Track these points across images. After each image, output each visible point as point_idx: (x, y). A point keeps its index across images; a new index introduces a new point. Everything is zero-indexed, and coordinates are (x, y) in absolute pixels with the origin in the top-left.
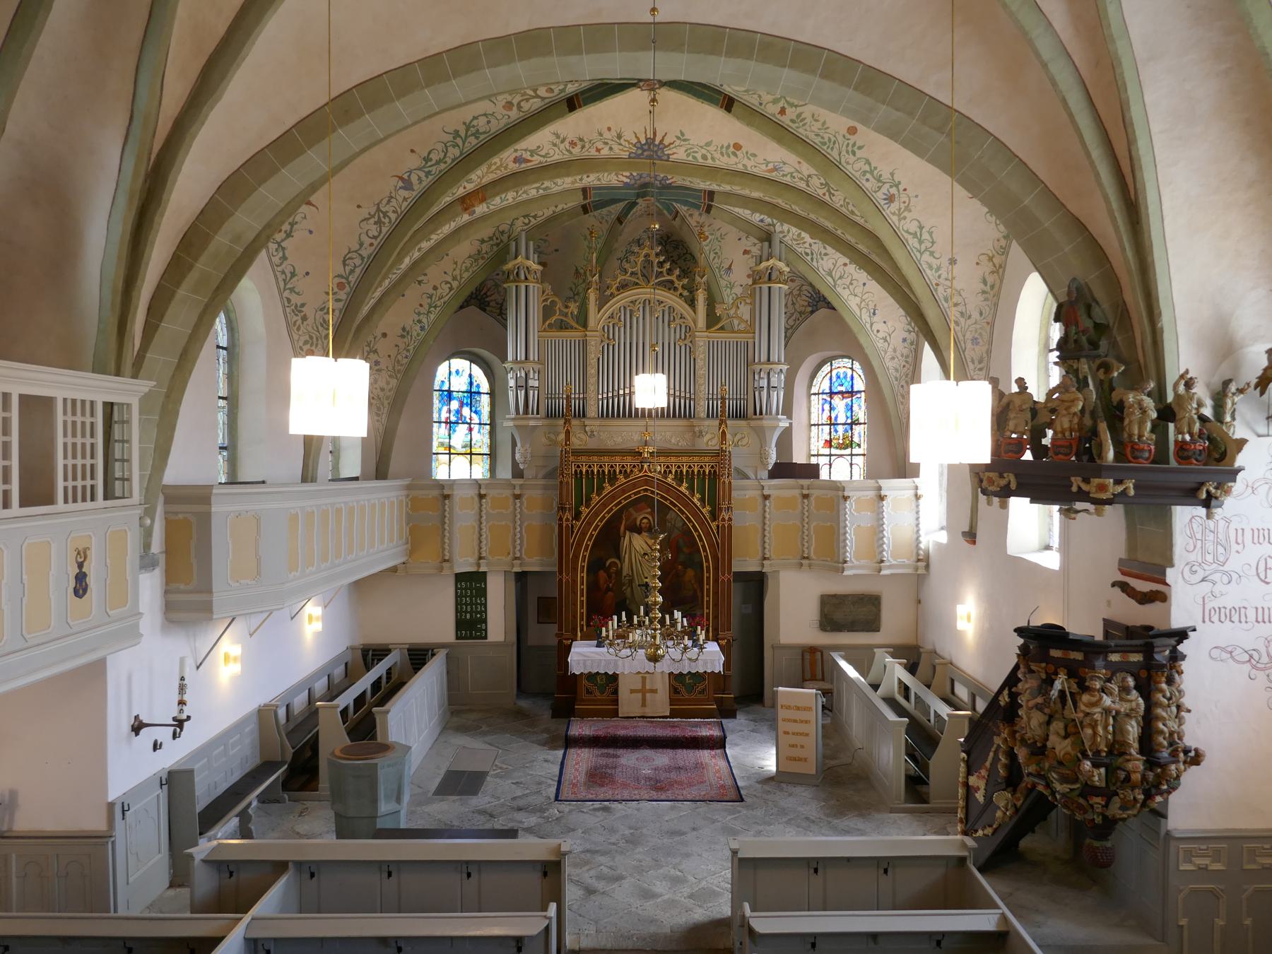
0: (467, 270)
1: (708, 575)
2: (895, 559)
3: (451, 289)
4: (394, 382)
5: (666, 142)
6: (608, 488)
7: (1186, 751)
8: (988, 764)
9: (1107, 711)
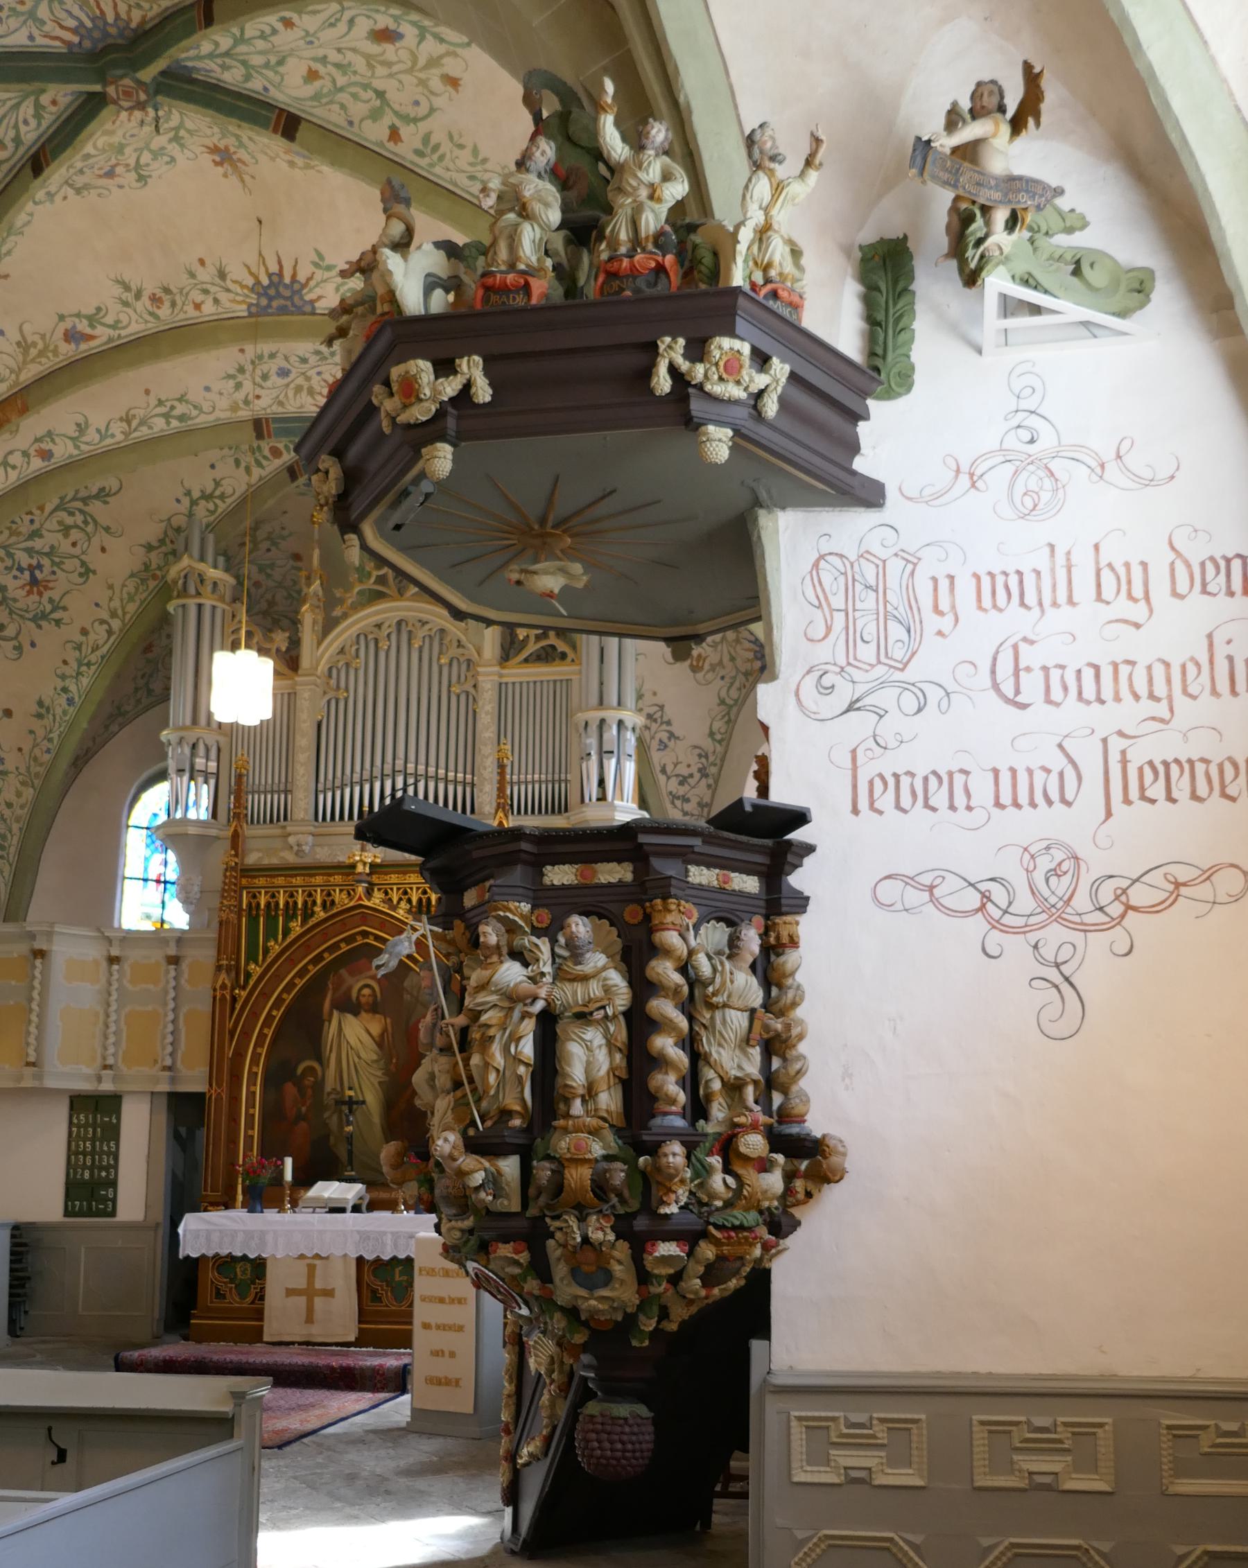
0: (131, 599)
3: (110, 632)
4: (29, 793)
5: (302, 277)
6: (296, 927)
9: (512, 998)
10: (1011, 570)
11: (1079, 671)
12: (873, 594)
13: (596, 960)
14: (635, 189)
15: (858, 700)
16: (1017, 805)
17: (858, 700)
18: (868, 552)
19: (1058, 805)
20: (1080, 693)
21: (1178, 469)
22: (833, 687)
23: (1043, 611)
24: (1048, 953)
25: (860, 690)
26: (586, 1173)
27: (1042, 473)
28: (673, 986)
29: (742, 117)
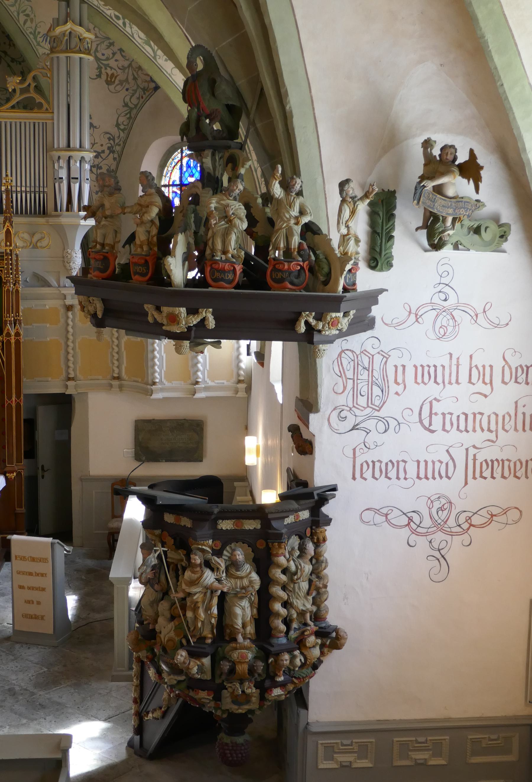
10: (431, 365)
11: (458, 416)
12: (367, 372)
13: (247, 568)
14: (289, 220)
15: (357, 425)
16: (427, 478)
17: (357, 425)
18: (365, 350)
19: (445, 479)
20: (458, 427)
21: (510, 321)
22: (346, 417)
23: (444, 386)
24: (435, 545)
25: (359, 419)
26: (246, 667)
27: (449, 317)
28: (283, 582)
29: (316, 115)
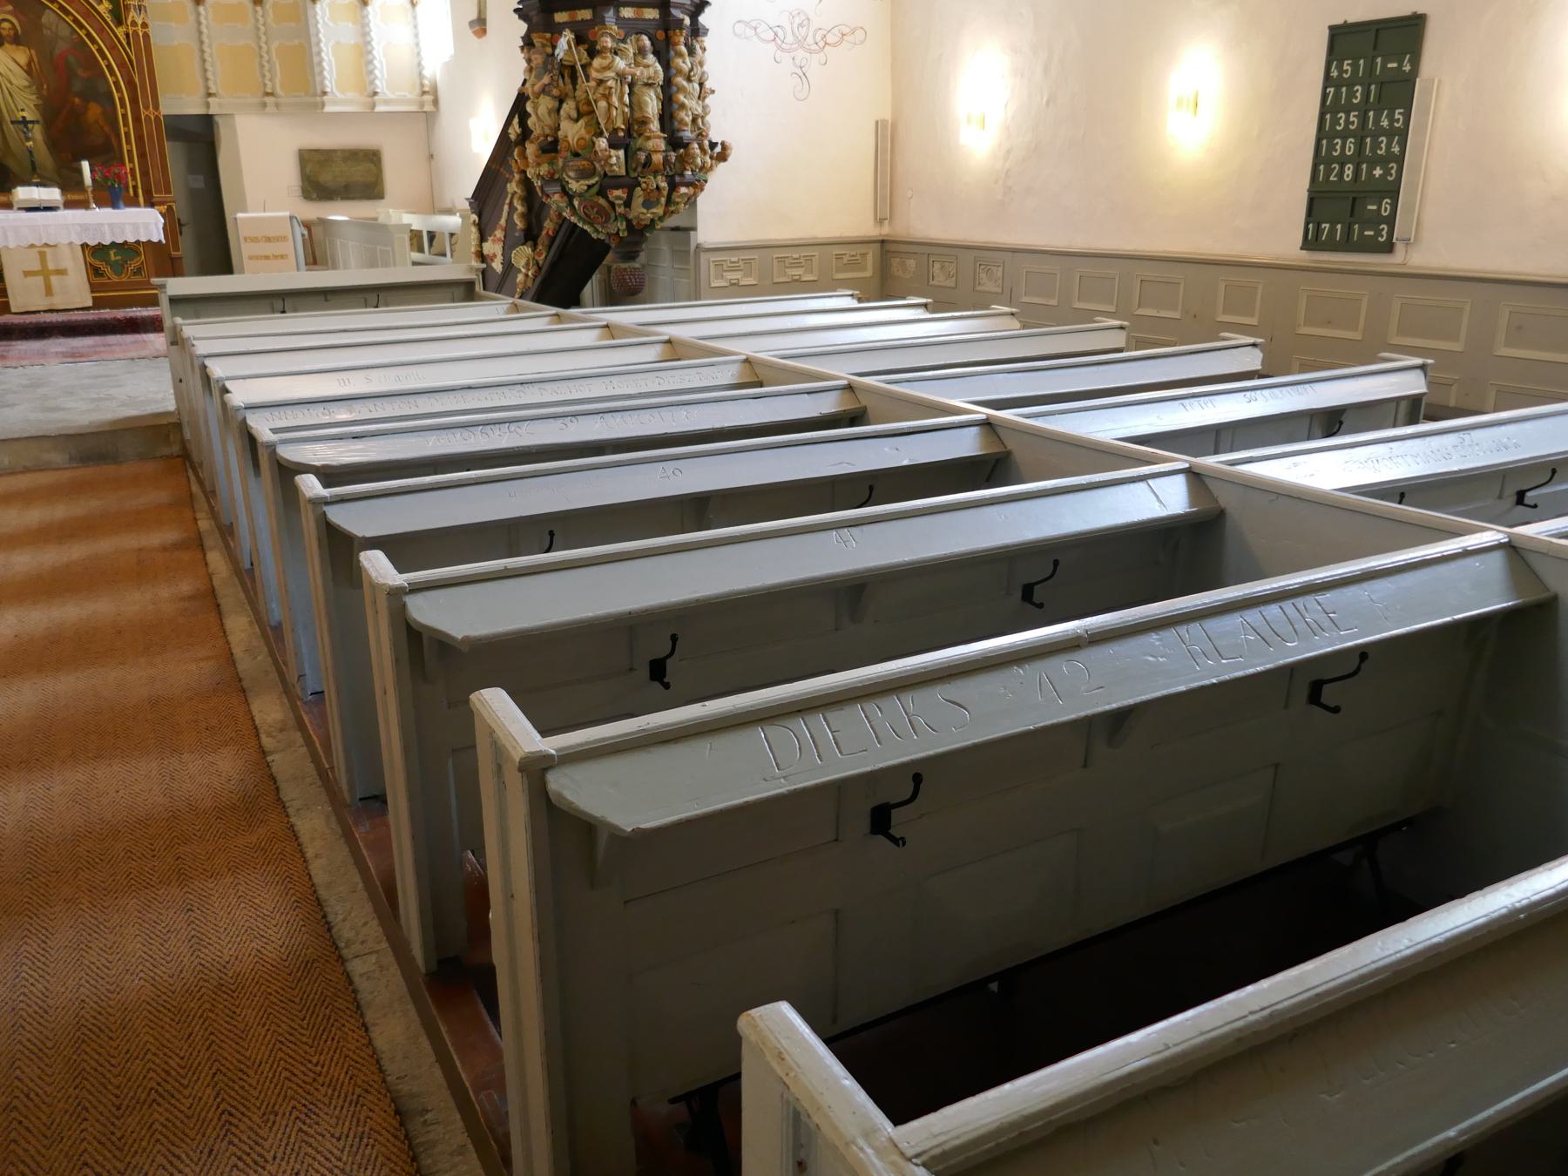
1: (124, 112)
2: (394, 91)
7: (713, 145)
8: (503, 222)
9: (621, 76)
